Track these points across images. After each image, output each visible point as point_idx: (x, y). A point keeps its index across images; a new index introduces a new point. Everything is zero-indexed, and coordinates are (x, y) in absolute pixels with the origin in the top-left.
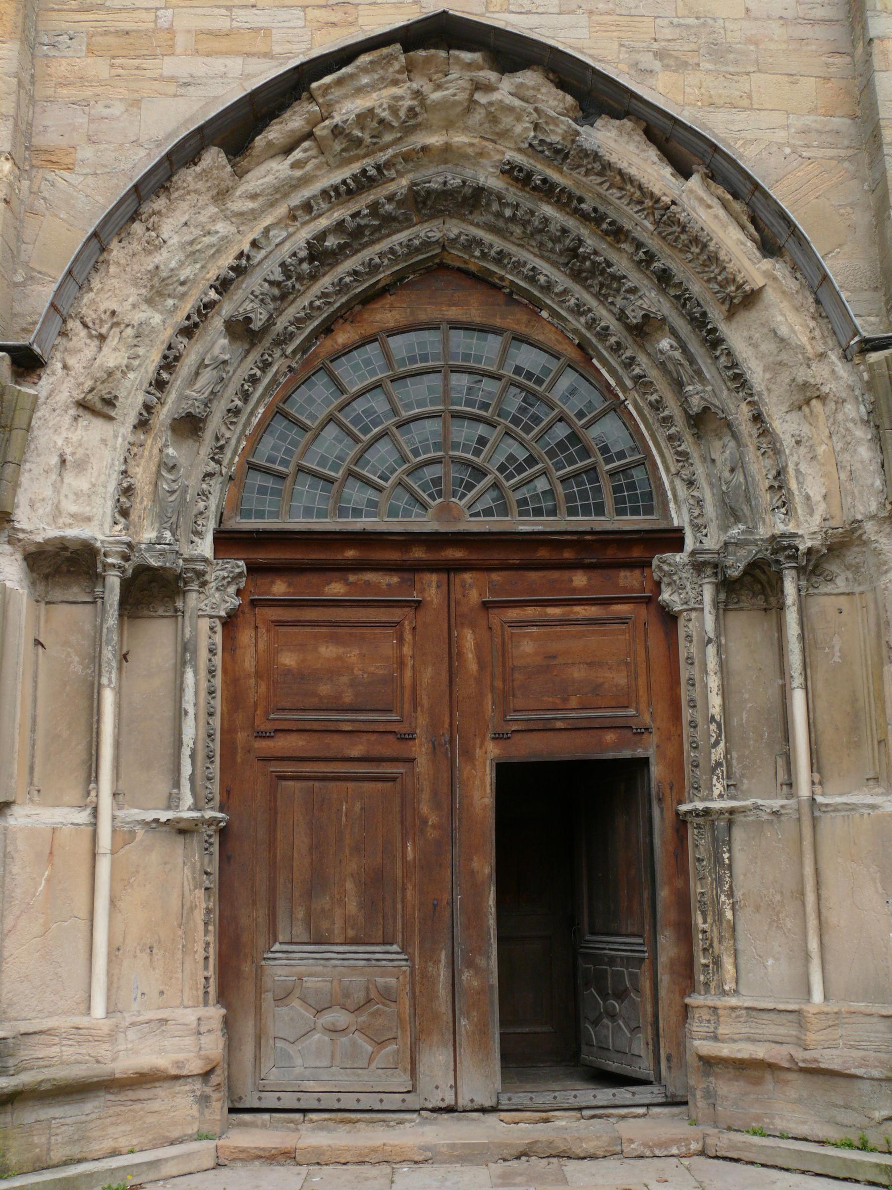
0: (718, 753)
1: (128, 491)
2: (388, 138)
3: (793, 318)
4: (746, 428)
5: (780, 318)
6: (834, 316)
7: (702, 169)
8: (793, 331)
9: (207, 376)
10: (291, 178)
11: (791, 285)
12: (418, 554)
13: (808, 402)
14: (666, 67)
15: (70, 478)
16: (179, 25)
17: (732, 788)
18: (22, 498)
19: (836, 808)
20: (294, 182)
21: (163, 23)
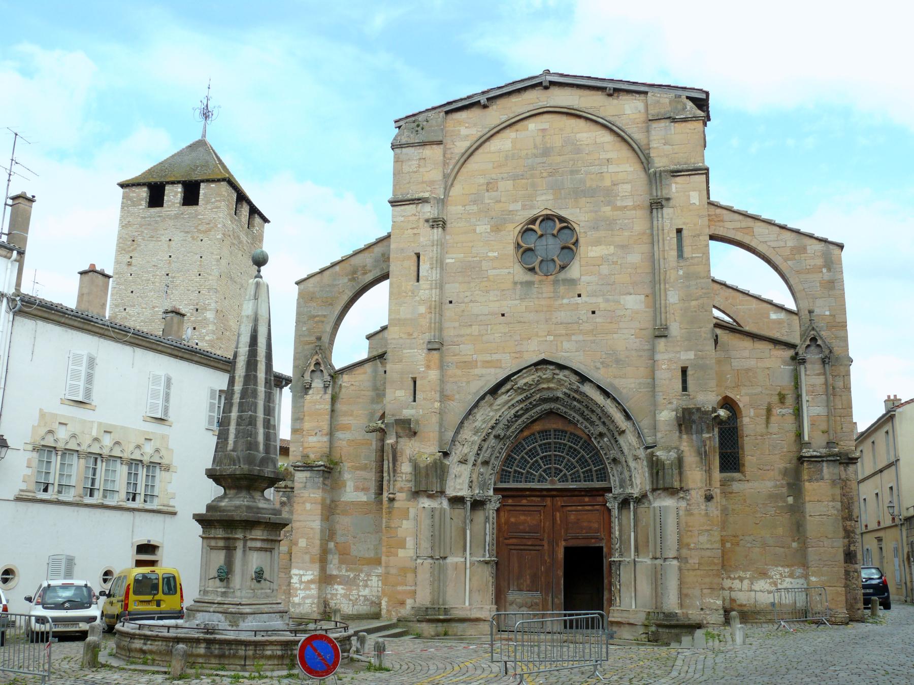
0: (617, 546)
1: (471, 482)
4: (624, 463)
9: (489, 450)
12: (545, 493)
17: (621, 555)
18: (447, 486)
19: (639, 562)
21: (474, 359)
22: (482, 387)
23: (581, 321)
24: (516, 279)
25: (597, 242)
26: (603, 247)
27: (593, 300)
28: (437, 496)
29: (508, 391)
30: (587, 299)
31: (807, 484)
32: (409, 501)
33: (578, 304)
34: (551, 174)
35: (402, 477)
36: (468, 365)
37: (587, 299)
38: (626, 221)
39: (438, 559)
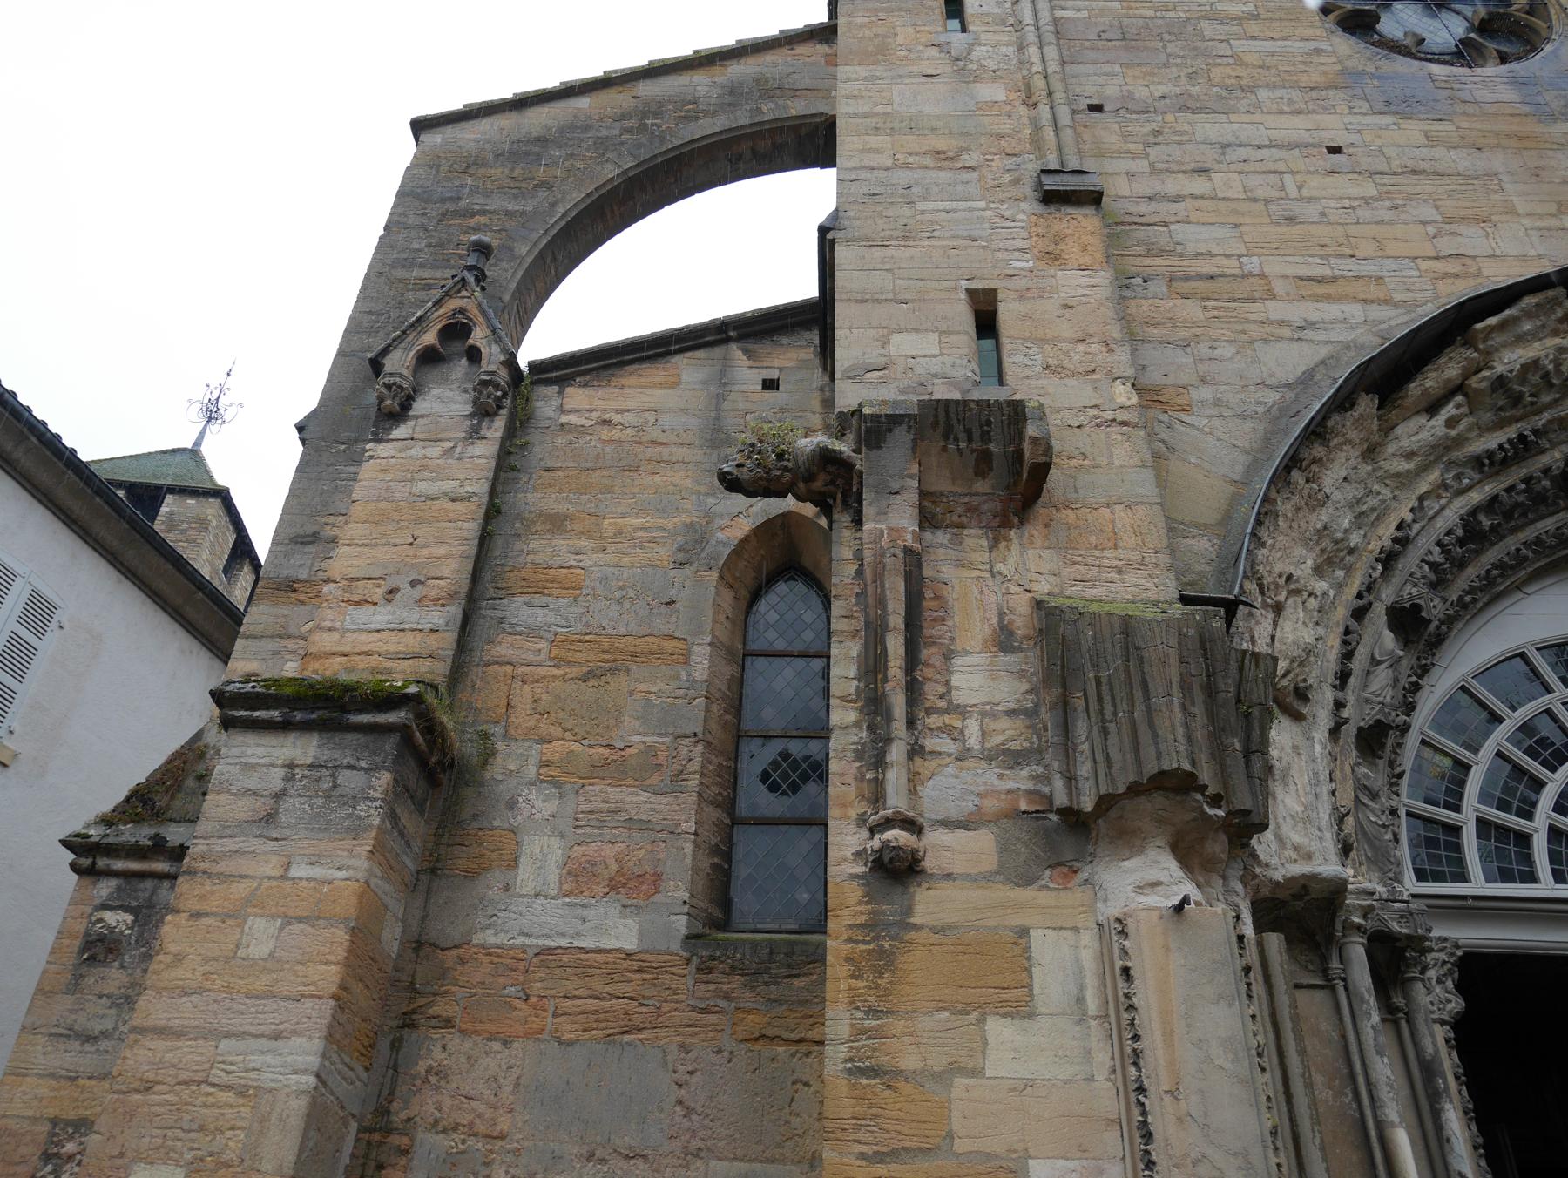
2: (1546, 398)
10: (1447, 437)
20: (1449, 443)
32: (1027, 881)
35: (957, 735)
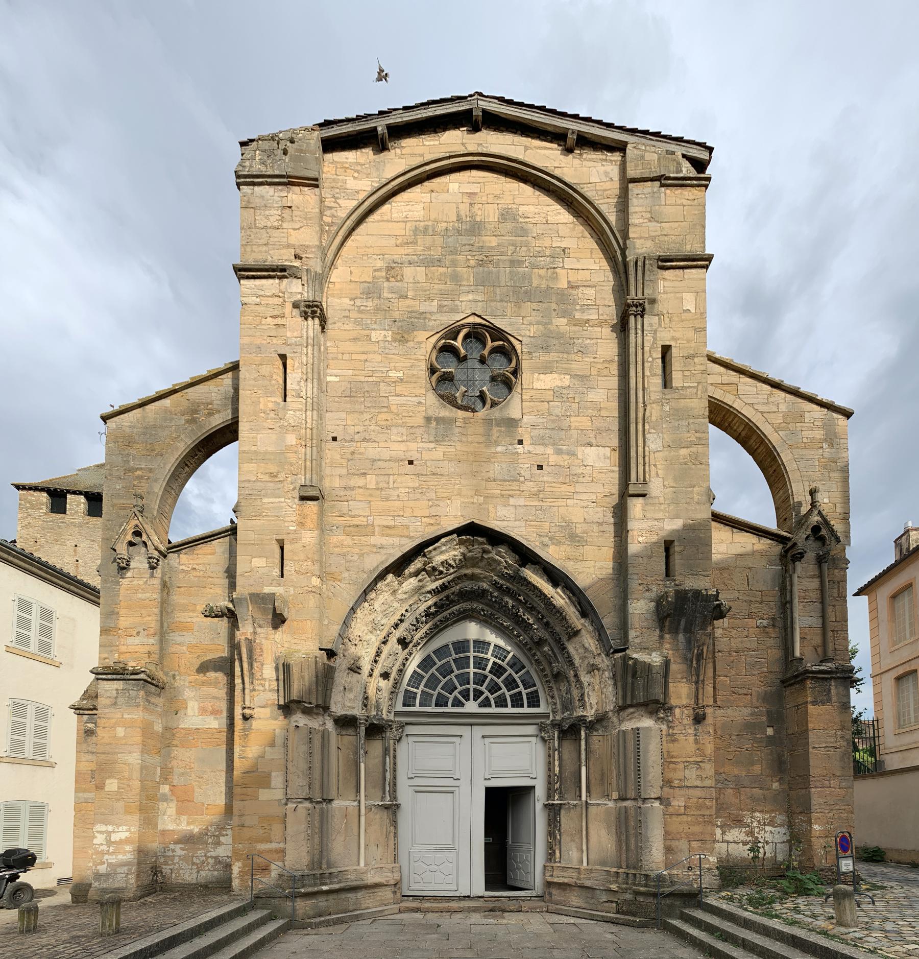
3: (591, 641)
5: (586, 641)
6: (605, 641)
7: (563, 584)
8: (590, 645)
11: (590, 628)
13: (593, 671)
14: (553, 544)
15: (347, 694)
16: (376, 523)
18: (332, 701)
19: (594, 805)
22: (382, 563)
23: (522, 479)
24: (430, 413)
25: (547, 369)
26: (555, 375)
27: (539, 449)
28: (317, 714)
29: (416, 574)
30: (531, 448)
31: (810, 706)
33: (517, 453)
34: (481, 264)
36: (364, 530)
37: (531, 448)
38: (588, 341)
39: (318, 803)
